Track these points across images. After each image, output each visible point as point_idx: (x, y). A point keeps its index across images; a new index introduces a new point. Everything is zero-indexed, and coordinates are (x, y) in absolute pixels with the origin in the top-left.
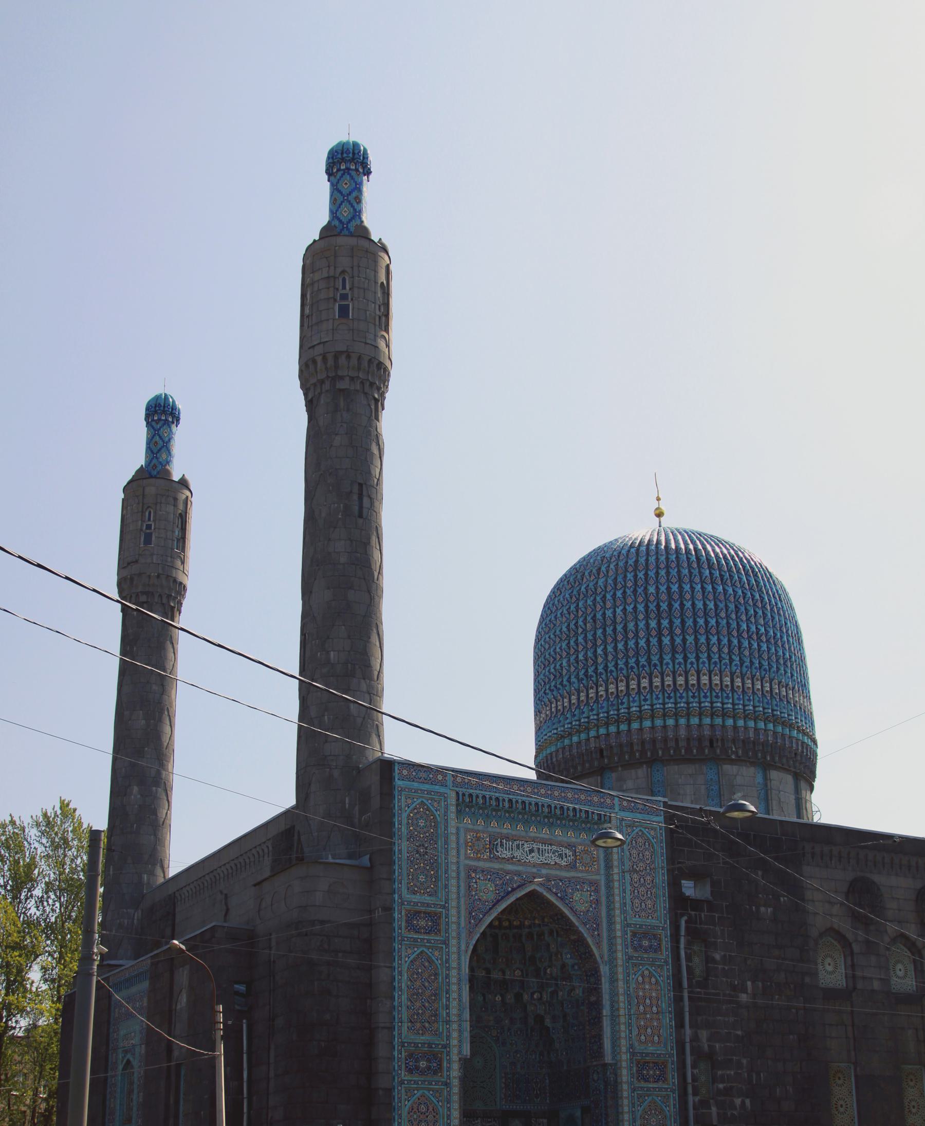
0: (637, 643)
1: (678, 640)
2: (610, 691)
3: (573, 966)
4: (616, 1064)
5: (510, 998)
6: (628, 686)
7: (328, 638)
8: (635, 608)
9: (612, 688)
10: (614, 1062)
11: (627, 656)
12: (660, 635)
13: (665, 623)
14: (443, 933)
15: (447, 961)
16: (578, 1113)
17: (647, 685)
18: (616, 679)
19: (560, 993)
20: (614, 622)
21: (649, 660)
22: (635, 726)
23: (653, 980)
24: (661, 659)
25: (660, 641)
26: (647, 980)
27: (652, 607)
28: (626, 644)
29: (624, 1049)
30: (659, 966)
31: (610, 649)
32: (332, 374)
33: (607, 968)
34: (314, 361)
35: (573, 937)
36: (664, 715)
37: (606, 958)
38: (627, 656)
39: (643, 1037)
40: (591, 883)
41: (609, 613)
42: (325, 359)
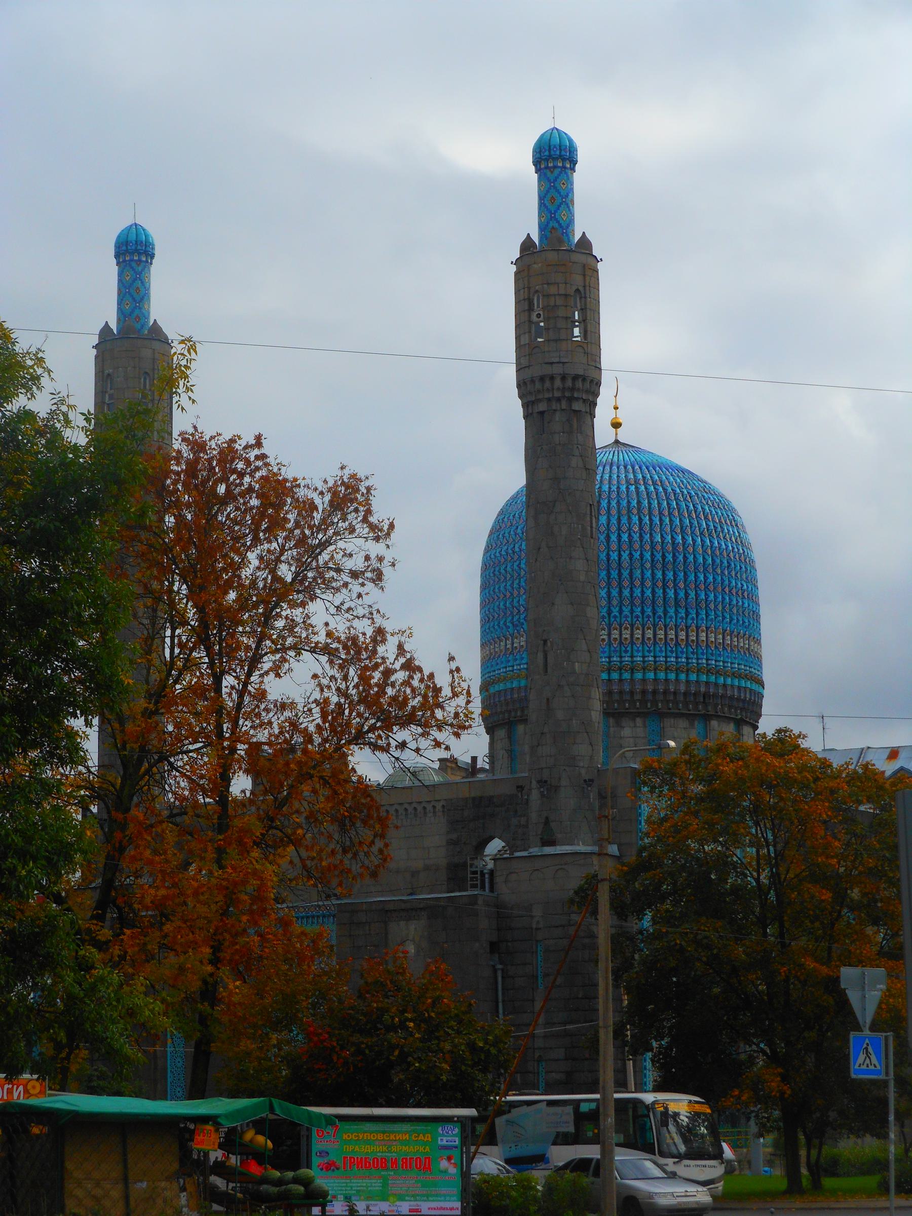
0: (643, 592)
1: (682, 594)
2: (613, 636)
6: (632, 635)
7: (573, 650)
8: (642, 556)
9: (615, 634)
11: (632, 604)
12: (665, 587)
13: (670, 575)
17: (651, 636)
18: (621, 625)
20: (620, 564)
21: (654, 612)
22: (639, 676)
24: (665, 612)
25: (664, 592)
27: (659, 556)
28: (632, 592)
31: (615, 593)
32: (567, 394)
34: (552, 378)
36: (667, 669)
38: (632, 604)
41: (614, 556)
42: (564, 378)
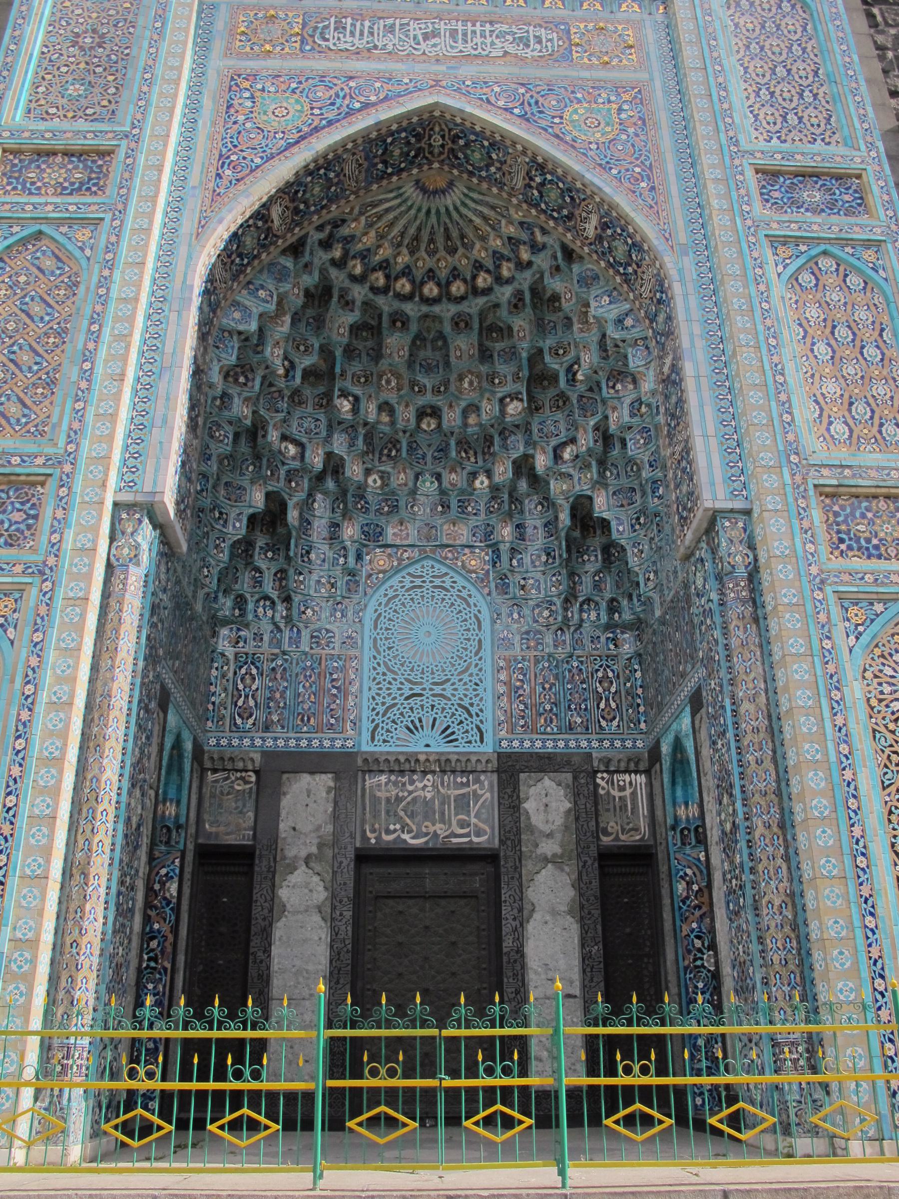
3: (619, 321)
4: (748, 513)
5: (503, 471)
10: (739, 505)
14: (112, 190)
15: (112, 248)
16: (686, 721)
19: (613, 417)
23: (854, 280)
26: (831, 280)
29: (767, 458)
30: (868, 244)
33: (688, 262)
35: (591, 228)
37: (682, 237)
39: (839, 428)
40: (618, 89)
